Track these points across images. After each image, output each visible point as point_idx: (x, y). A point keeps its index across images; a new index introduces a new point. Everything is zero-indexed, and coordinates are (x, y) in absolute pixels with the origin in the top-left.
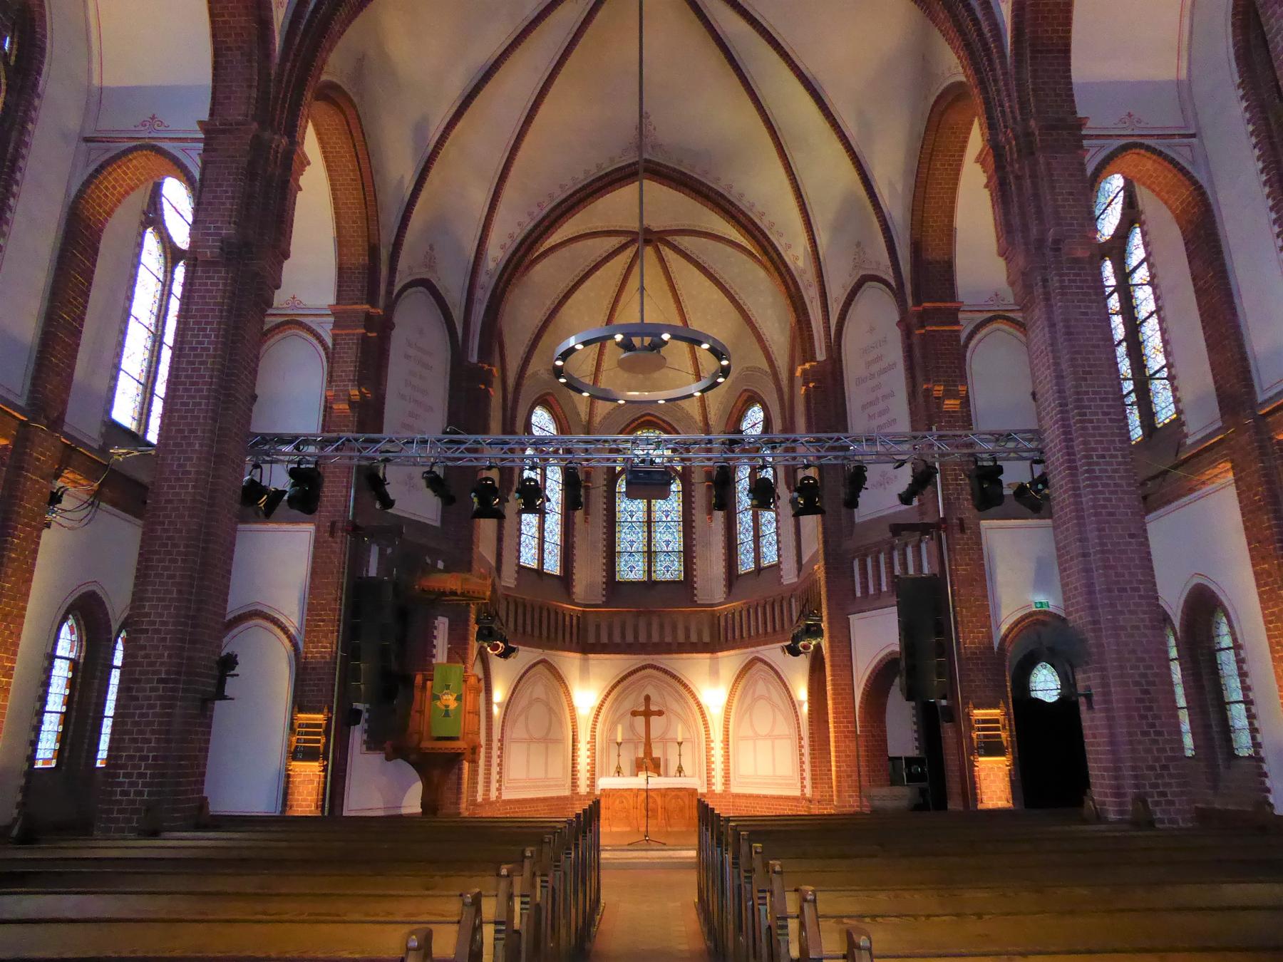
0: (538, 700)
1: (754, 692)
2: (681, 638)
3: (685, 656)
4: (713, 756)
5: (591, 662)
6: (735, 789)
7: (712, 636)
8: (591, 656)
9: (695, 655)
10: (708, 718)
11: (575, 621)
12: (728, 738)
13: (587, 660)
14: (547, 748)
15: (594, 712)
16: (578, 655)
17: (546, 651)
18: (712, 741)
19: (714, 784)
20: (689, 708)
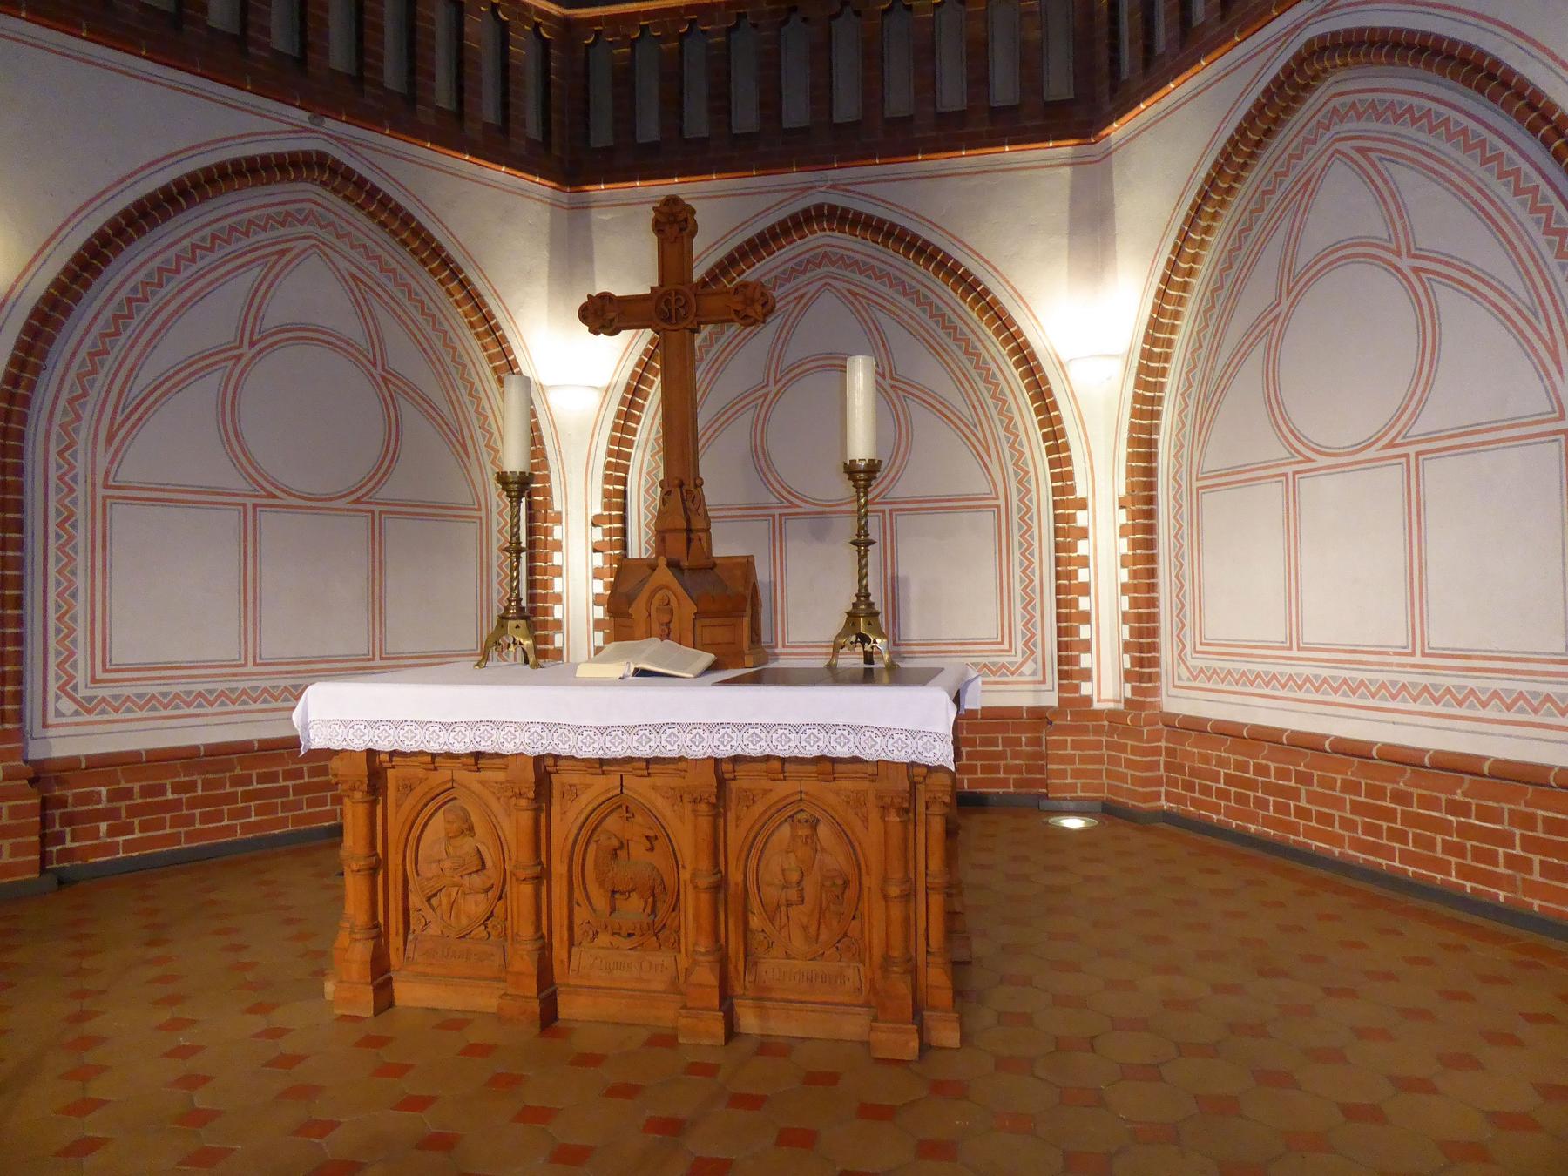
0: (301, 333)
1: (1293, 242)
2: (952, 96)
3: (965, 159)
4: (1084, 562)
5: (599, 216)
6: (1177, 700)
7: (1083, 72)
8: (600, 190)
9: (1011, 154)
10: (1065, 411)
11: (522, 51)
12: (1151, 486)
13: (585, 207)
14: (376, 537)
15: (614, 406)
16: (538, 186)
17: (330, 124)
18: (1082, 505)
19: (1086, 675)
20: (990, 379)
